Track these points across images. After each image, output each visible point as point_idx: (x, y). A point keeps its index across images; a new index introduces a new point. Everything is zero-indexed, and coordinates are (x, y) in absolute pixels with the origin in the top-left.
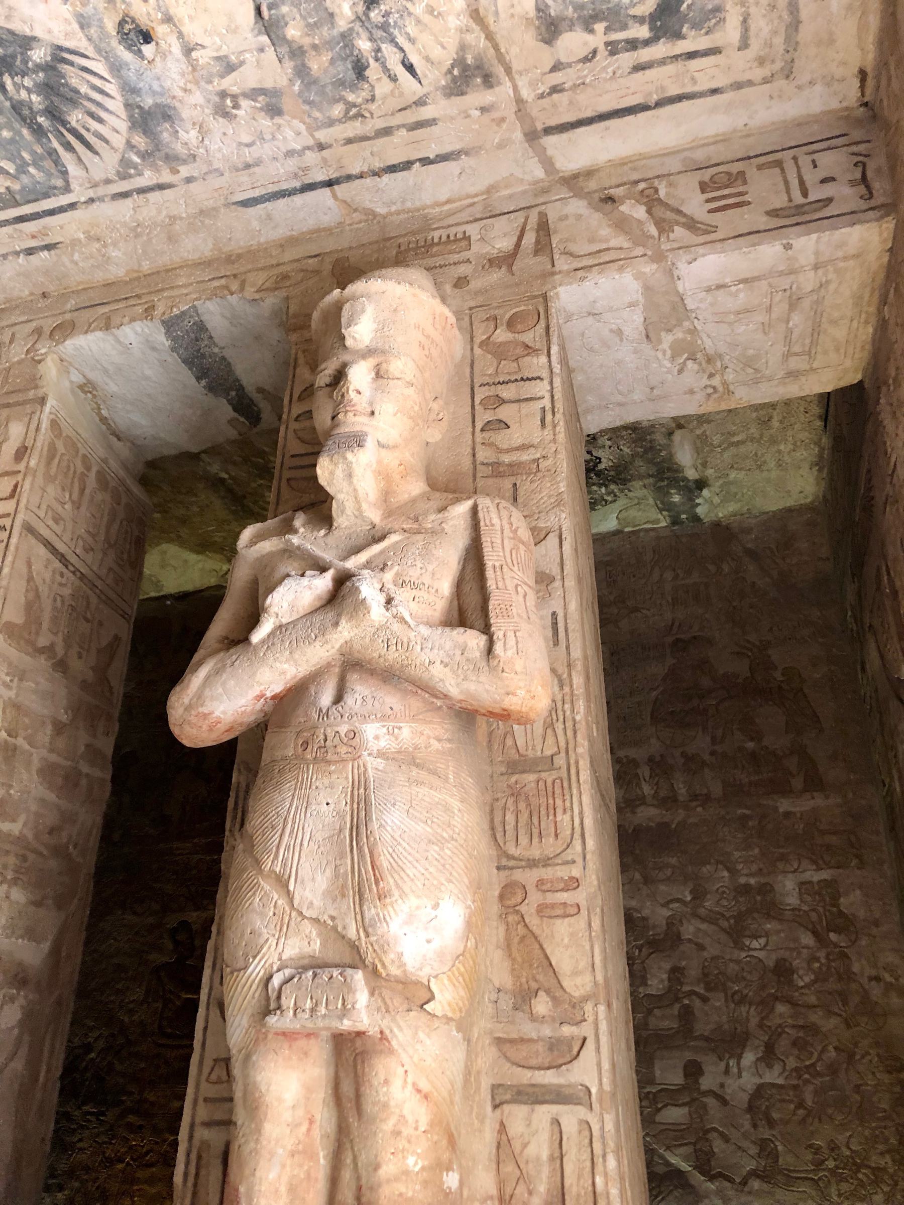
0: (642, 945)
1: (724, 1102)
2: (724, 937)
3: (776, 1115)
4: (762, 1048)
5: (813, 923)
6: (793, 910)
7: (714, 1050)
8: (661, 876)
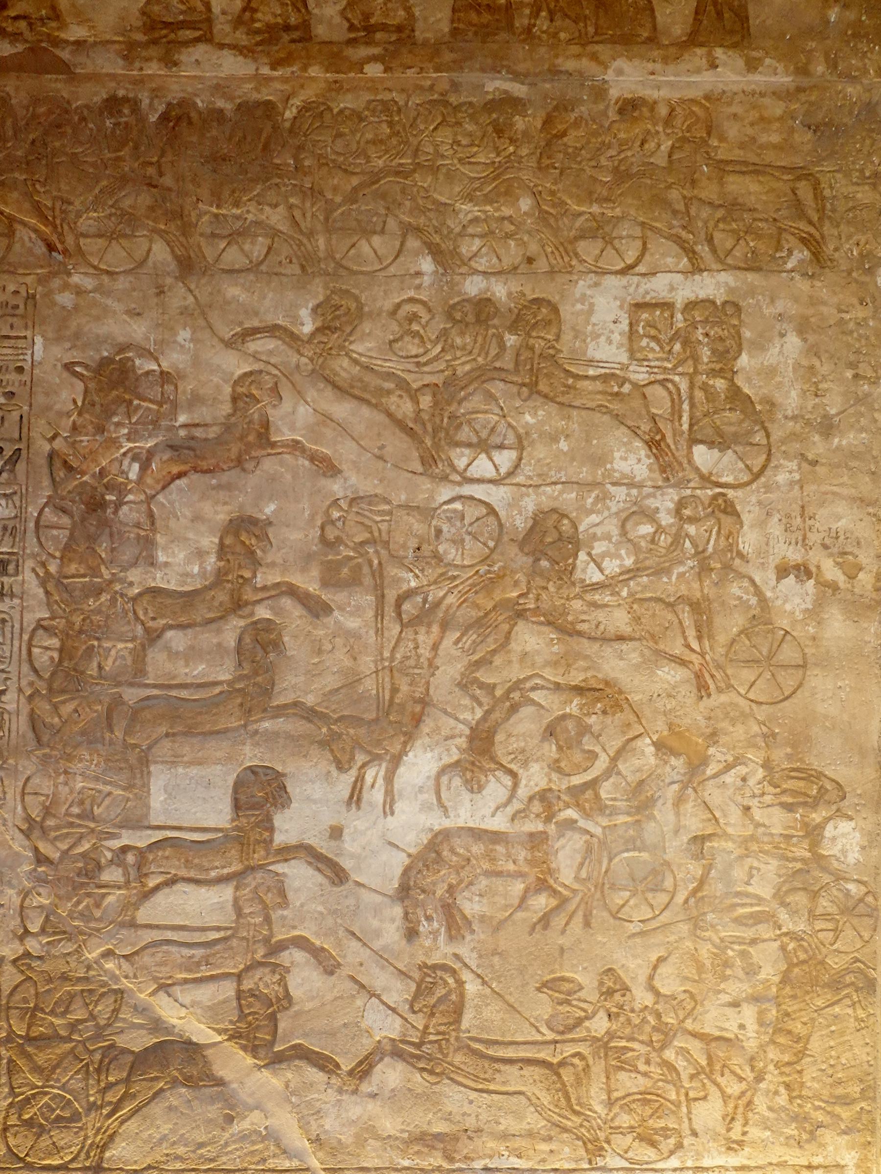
0: (151, 453)
1: (337, 874)
2: (396, 444)
3: (471, 906)
4: (462, 742)
5: (653, 418)
6: (605, 378)
7: (324, 744)
8: (233, 257)
